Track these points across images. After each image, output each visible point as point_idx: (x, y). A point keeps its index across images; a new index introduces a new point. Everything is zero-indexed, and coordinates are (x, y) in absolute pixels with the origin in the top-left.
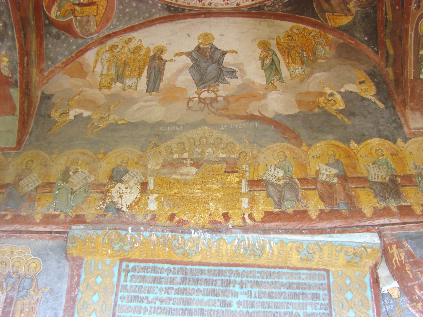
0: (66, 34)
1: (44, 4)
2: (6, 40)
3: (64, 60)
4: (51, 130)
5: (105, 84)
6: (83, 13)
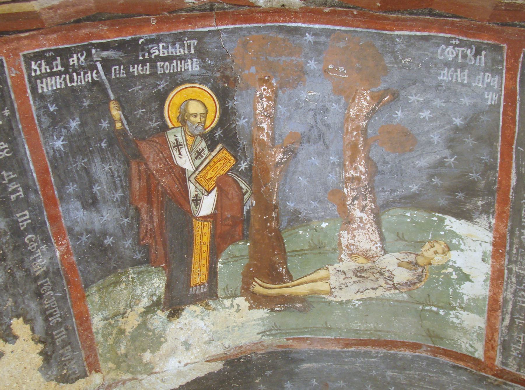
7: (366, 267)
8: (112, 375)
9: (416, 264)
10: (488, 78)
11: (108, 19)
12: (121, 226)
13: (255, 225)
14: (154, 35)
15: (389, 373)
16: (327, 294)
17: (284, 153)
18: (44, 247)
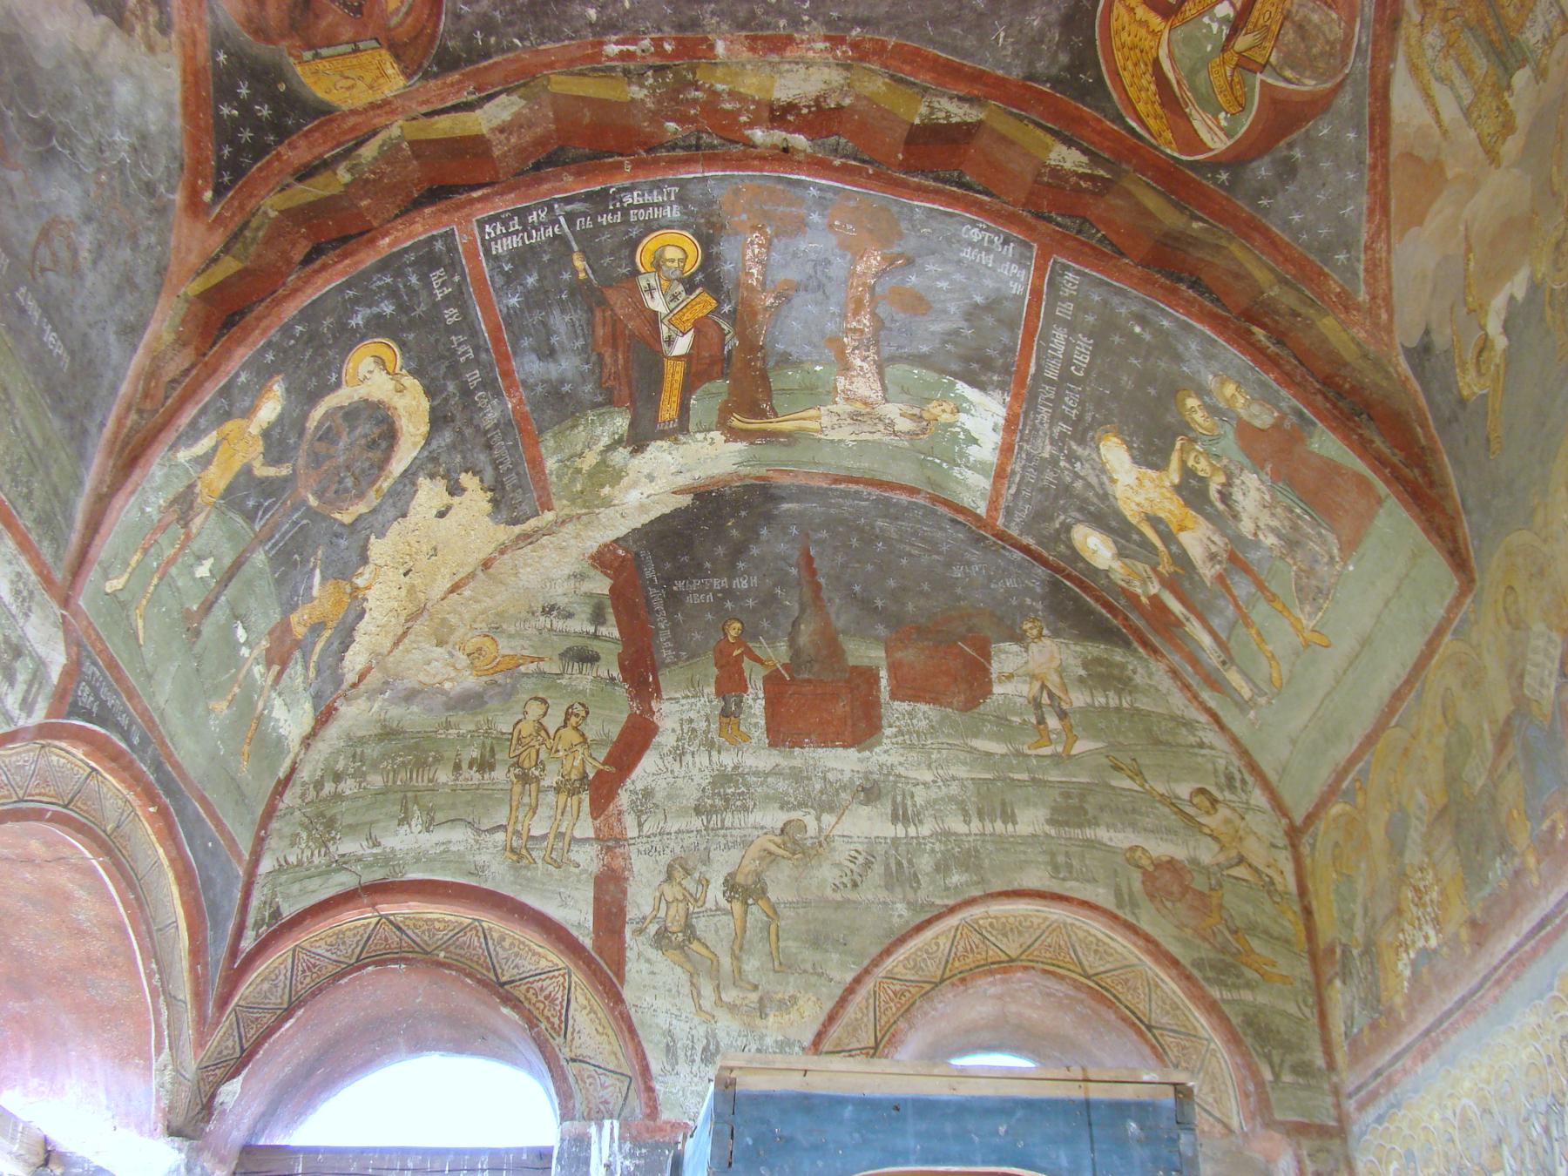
0: (1295, 136)
1: (1169, 151)
2: (1181, 348)
3: (1364, 200)
4: (1488, 440)
5: (1492, 131)
6: (1268, 28)
7: (863, 412)
8: (567, 511)
9: (921, 417)
10: (1015, 269)
11: (574, 161)
12: (582, 374)
13: (737, 364)
14: (627, 184)
15: (879, 523)
16: (817, 431)
17: (775, 298)
18: (495, 402)
